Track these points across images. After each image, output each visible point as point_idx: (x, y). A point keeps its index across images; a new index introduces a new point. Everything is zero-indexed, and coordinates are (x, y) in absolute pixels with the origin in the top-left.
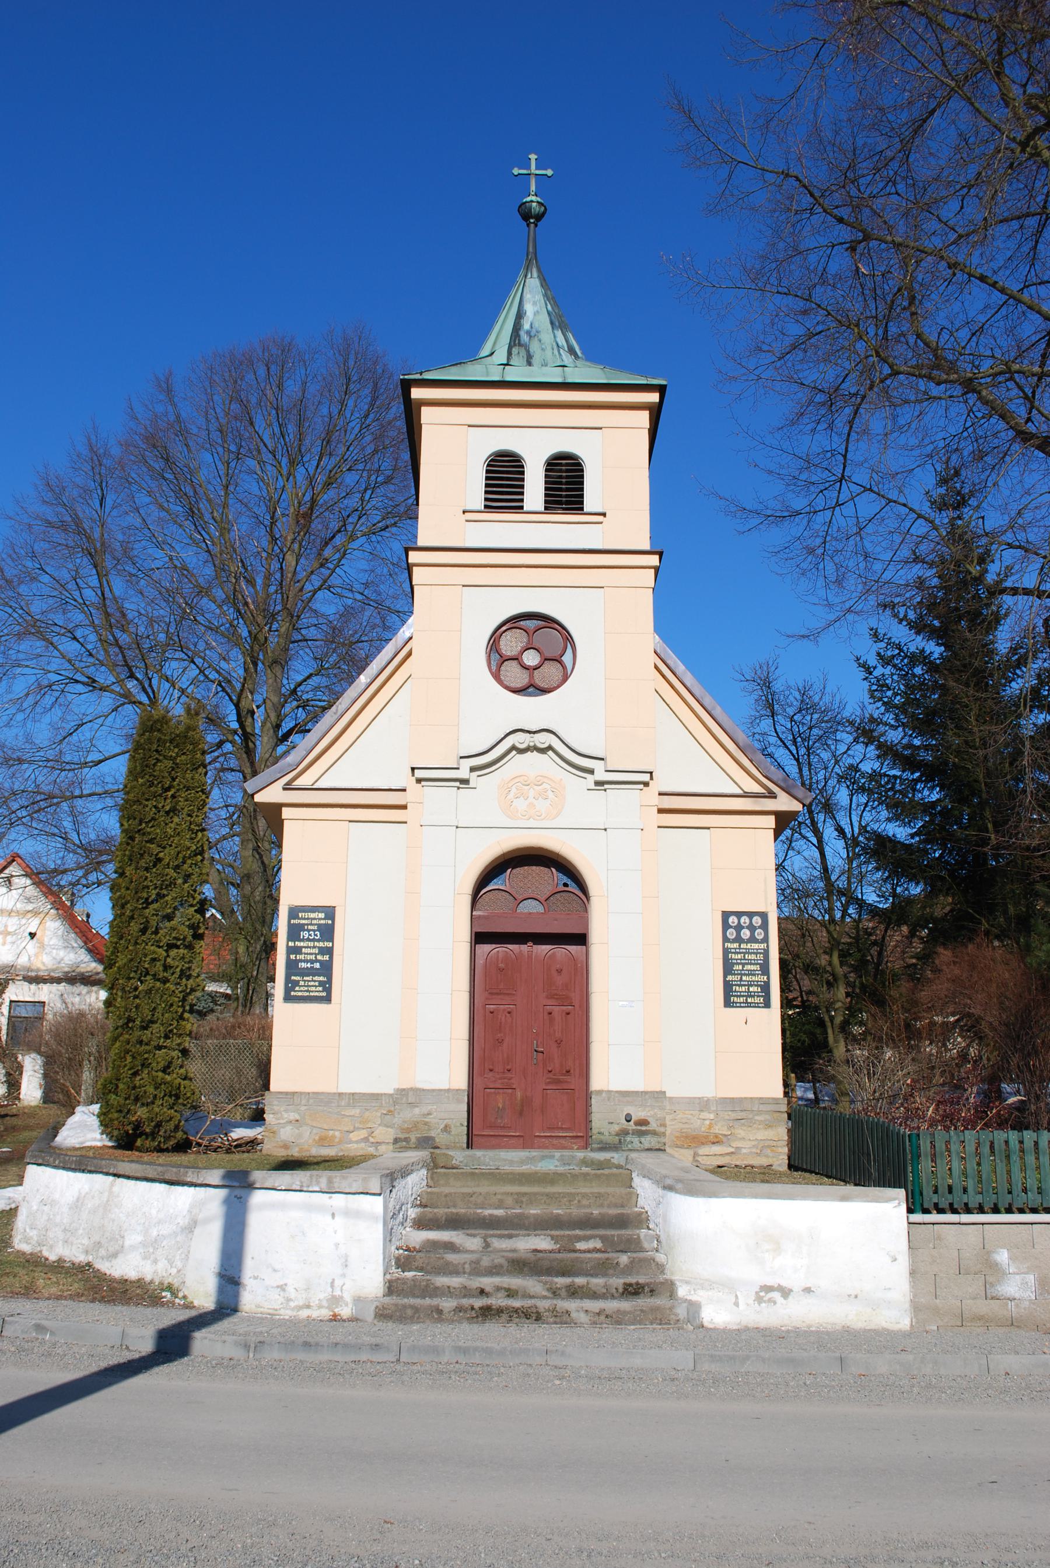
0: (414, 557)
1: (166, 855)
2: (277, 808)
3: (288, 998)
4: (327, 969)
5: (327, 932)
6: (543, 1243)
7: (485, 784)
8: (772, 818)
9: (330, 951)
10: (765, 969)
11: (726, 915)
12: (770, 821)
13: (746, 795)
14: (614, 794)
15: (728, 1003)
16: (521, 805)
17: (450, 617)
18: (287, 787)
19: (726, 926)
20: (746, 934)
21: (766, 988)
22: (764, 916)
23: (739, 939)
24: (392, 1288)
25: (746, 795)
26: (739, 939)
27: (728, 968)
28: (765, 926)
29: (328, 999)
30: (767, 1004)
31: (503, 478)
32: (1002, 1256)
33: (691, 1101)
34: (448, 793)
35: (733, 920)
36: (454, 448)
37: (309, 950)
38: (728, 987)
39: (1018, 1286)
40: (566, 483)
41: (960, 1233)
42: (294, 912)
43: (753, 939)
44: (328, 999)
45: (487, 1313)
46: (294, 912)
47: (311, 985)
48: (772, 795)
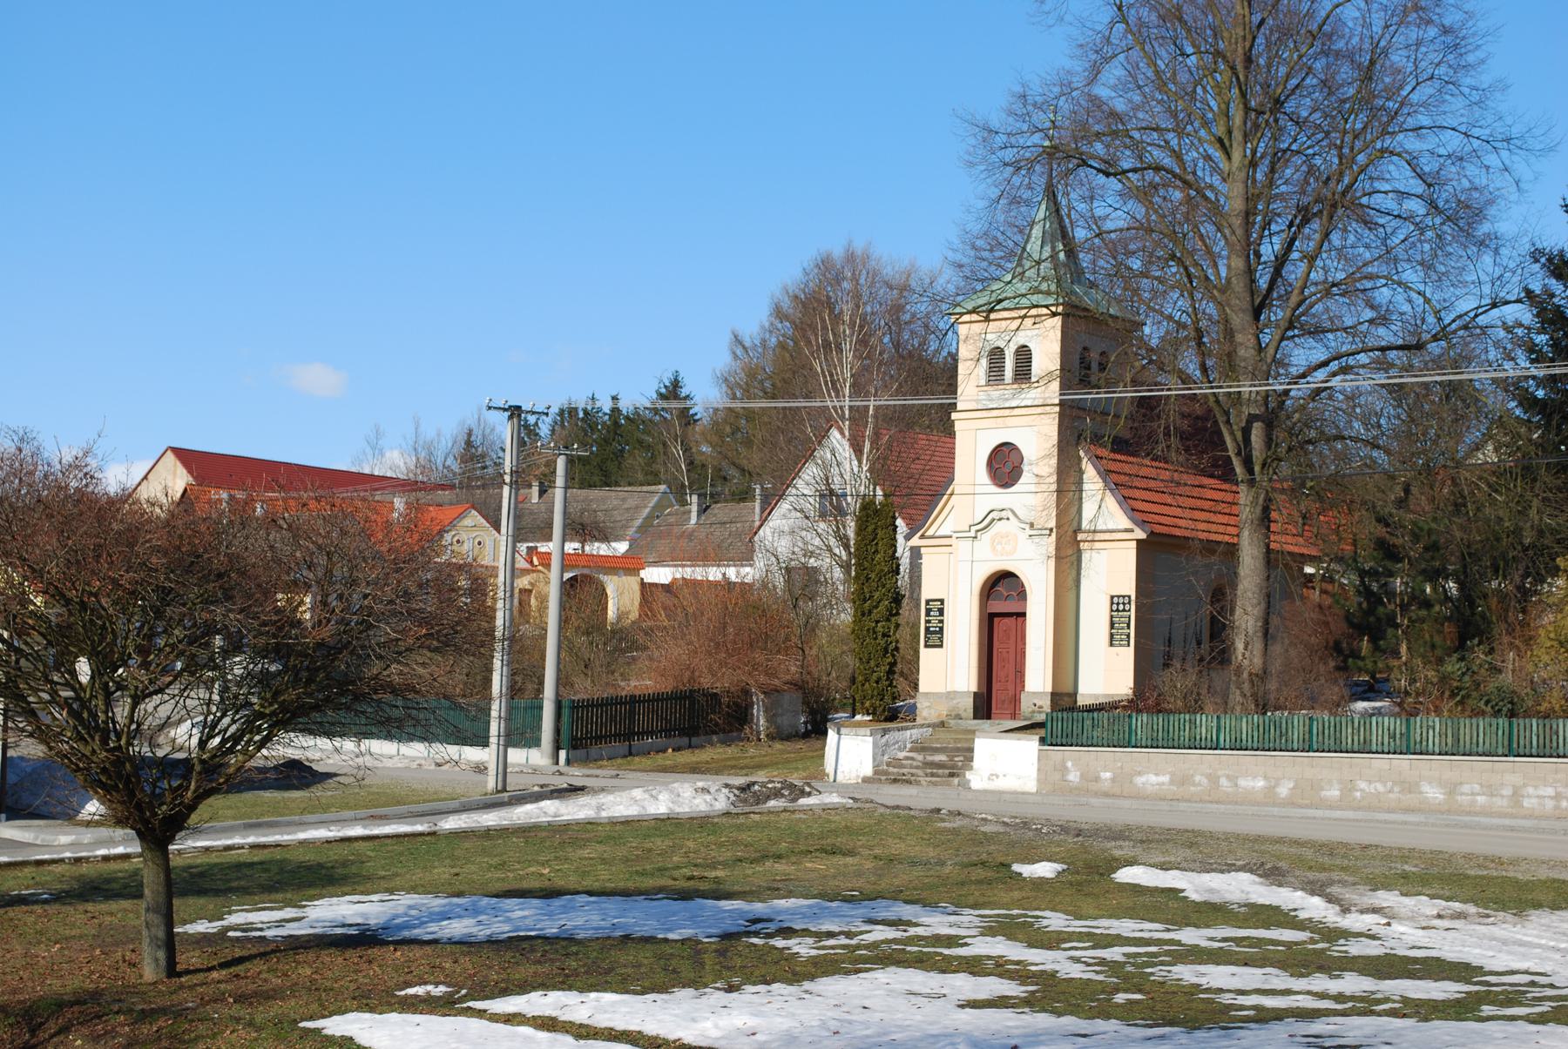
1: (873, 576)
3: (926, 646)
4: (941, 629)
5: (941, 612)
6: (942, 758)
7: (985, 537)
13: (1127, 530)
16: (999, 547)
18: (922, 537)
24: (876, 772)
25: (1127, 530)
27: (1112, 625)
32: (1069, 764)
37: (934, 622)
38: (1112, 635)
39: (1074, 777)
41: (1057, 753)
42: (928, 602)
45: (895, 781)
46: (928, 602)
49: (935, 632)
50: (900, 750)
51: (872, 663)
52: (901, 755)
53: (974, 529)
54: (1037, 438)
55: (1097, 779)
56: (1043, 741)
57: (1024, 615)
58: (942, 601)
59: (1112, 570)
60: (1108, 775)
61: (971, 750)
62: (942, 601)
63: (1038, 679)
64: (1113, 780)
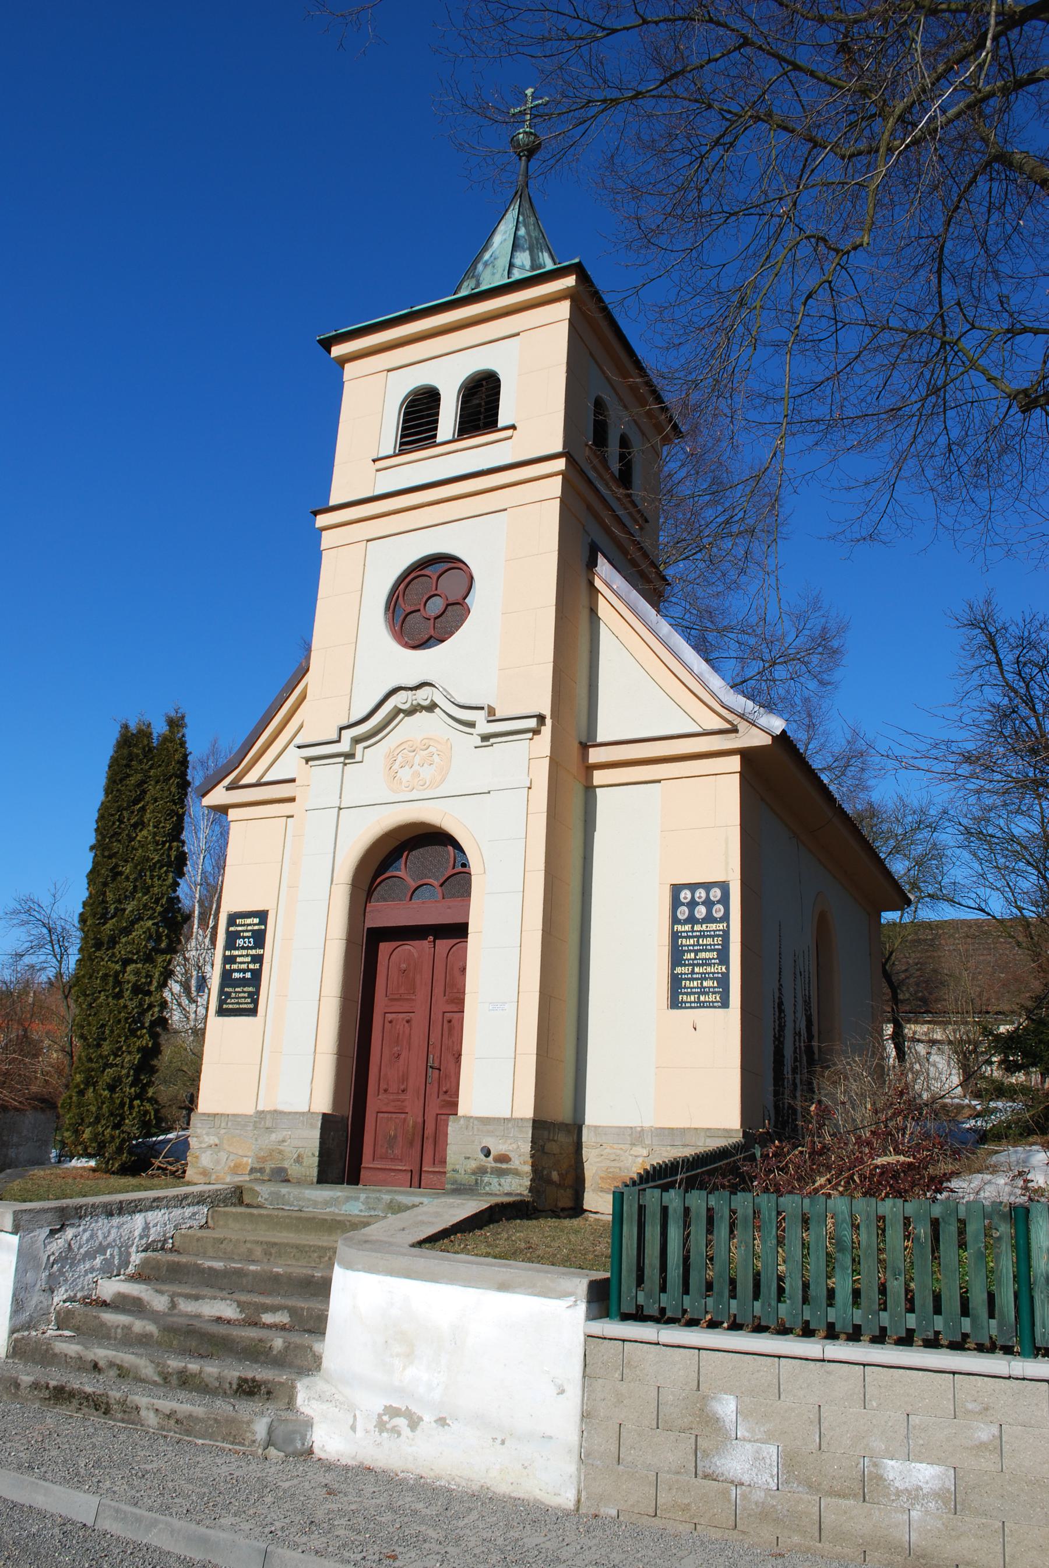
0: (322, 520)
1: (127, 869)
2: (223, 810)
3: (221, 1012)
4: (257, 975)
5: (259, 939)
6: (222, 1308)
7: (374, 756)
8: (737, 759)
9: (259, 959)
10: (724, 957)
11: (676, 889)
12: (734, 763)
14: (501, 749)
15: (675, 1003)
16: (405, 774)
17: (356, 573)
18: (232, 787)
19: (676, 903)
20: (701, 911)
21: (724, 981)
22: (724, 887)
23: (692, 920)
26: (692, 920)
27: (677, 956)
28: (725, 900)
29: (253, 1012)
30: (725, 1004)
31: (419, 417)
32: (727, 1407)
33: (621, 1132)
34: (332, 771)
35: (685, 895)
36: (371, 394)
37: (243, 958)
38: (676, 983)
39: (748, 1462)
40: (481, 405)
41: (669, 1354)
42: (232, 919)
43: (709, 919)
44: (253, 1012)
45: (60, 1395)
46: (232, 919)
47: (240, 996)
48: (734, 730)
49: (243, 982)
50: (109, 1271)
51: (106, 1048)
52: (109, 1288)
53: (348, 735)
54: (513, 541)
55: (867, 1487)
56: (602, 1300)
57: (459, 931)
58: (262, 916)
59: (678, 833)
60: (926, 1474)
61: (322, 1288)
62: (262, 916)
63: (495, 1082)
64: (956, 1500)
